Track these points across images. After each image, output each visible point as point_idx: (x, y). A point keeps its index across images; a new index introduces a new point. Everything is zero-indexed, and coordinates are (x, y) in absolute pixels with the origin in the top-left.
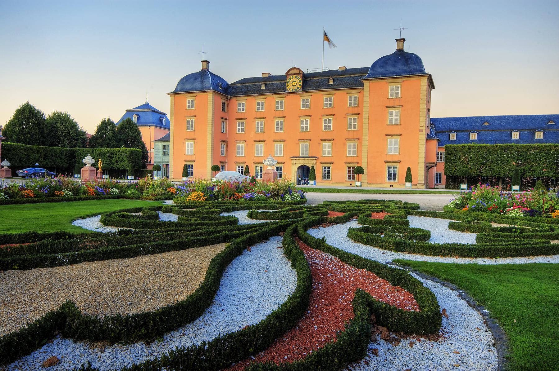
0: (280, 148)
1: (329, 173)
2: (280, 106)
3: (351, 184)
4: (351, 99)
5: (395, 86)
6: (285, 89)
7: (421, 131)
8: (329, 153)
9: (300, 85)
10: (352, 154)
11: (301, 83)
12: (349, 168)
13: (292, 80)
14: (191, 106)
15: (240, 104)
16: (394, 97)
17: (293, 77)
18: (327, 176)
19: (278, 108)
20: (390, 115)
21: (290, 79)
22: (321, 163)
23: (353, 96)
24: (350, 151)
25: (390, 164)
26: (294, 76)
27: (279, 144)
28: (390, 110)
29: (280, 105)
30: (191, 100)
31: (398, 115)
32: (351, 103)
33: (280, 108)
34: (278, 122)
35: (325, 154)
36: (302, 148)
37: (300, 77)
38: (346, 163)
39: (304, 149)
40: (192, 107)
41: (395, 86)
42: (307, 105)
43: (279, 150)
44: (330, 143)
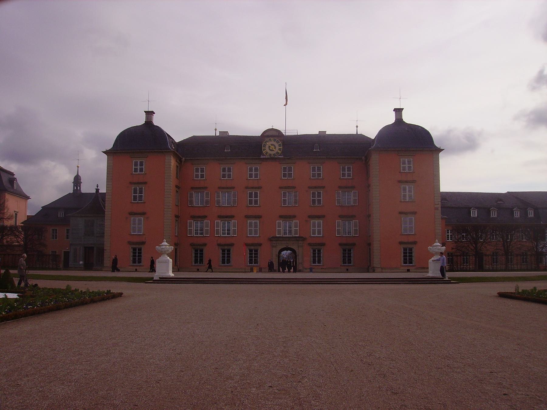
0: (256, 226)
1: (319, 257)
2: (254, 174)
3: (347, 270)
4: (344, 169)
5: (406, 160)
6: (261, 153)
7: (436, 209)
8: (319, 233)
9: (280, 149)
10: (317, 234)
12: (344, 250)
14: (139, 169)
16: (407, 171)
17: (270, 140)
18: (317, 260)
19: (251, 176)
20: (403, 190)
22: (310, 244)
23: (346, 167)
25: (405, 246)
27: (253, 221)
29: (253, 173)
30: (139, 161)
31: (412, 191)
32: (344, 175)
33: (254, 177)
35: (314, 233)
37: (280, 140)
38: (340, 245)
41: (406, 160)
42: (290, 175)
43: (253, 229)
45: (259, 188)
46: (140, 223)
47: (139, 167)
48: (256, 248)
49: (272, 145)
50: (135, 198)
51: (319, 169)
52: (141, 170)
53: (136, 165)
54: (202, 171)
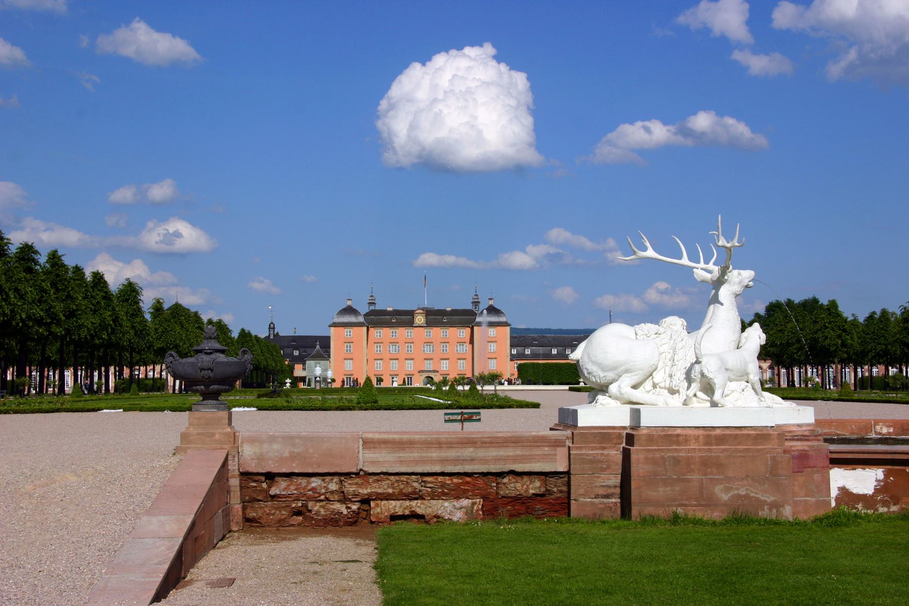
0: (411, 364)
4: (460, 332)
6: (413, 323)
8: (446, 368)
11: (425, 320)
13: (418, 317)
15: (377, 333)
17: (419, 316)
19: (408, 336)
21: (416, 317)
22: (441, 375)
24: (446, 364)
26: (420, 315)
28: (490, 344)
32: (460, 335)
34: (408, 346)
35: (443, 368)
36: (427, 365)
39: (428, 366)
40: (350, 335)
42: (430, 335)
44: (447, 361)
45: (413, 343)
46: (350, 364)
47: (348, 334)
48: (411, 376)
49: (421, 319)
50: (347, 350)
51: (446, 332)
52: (350, 335)
53: (347, 332)
54: (380, 333)
